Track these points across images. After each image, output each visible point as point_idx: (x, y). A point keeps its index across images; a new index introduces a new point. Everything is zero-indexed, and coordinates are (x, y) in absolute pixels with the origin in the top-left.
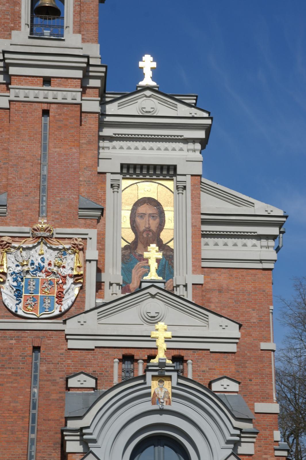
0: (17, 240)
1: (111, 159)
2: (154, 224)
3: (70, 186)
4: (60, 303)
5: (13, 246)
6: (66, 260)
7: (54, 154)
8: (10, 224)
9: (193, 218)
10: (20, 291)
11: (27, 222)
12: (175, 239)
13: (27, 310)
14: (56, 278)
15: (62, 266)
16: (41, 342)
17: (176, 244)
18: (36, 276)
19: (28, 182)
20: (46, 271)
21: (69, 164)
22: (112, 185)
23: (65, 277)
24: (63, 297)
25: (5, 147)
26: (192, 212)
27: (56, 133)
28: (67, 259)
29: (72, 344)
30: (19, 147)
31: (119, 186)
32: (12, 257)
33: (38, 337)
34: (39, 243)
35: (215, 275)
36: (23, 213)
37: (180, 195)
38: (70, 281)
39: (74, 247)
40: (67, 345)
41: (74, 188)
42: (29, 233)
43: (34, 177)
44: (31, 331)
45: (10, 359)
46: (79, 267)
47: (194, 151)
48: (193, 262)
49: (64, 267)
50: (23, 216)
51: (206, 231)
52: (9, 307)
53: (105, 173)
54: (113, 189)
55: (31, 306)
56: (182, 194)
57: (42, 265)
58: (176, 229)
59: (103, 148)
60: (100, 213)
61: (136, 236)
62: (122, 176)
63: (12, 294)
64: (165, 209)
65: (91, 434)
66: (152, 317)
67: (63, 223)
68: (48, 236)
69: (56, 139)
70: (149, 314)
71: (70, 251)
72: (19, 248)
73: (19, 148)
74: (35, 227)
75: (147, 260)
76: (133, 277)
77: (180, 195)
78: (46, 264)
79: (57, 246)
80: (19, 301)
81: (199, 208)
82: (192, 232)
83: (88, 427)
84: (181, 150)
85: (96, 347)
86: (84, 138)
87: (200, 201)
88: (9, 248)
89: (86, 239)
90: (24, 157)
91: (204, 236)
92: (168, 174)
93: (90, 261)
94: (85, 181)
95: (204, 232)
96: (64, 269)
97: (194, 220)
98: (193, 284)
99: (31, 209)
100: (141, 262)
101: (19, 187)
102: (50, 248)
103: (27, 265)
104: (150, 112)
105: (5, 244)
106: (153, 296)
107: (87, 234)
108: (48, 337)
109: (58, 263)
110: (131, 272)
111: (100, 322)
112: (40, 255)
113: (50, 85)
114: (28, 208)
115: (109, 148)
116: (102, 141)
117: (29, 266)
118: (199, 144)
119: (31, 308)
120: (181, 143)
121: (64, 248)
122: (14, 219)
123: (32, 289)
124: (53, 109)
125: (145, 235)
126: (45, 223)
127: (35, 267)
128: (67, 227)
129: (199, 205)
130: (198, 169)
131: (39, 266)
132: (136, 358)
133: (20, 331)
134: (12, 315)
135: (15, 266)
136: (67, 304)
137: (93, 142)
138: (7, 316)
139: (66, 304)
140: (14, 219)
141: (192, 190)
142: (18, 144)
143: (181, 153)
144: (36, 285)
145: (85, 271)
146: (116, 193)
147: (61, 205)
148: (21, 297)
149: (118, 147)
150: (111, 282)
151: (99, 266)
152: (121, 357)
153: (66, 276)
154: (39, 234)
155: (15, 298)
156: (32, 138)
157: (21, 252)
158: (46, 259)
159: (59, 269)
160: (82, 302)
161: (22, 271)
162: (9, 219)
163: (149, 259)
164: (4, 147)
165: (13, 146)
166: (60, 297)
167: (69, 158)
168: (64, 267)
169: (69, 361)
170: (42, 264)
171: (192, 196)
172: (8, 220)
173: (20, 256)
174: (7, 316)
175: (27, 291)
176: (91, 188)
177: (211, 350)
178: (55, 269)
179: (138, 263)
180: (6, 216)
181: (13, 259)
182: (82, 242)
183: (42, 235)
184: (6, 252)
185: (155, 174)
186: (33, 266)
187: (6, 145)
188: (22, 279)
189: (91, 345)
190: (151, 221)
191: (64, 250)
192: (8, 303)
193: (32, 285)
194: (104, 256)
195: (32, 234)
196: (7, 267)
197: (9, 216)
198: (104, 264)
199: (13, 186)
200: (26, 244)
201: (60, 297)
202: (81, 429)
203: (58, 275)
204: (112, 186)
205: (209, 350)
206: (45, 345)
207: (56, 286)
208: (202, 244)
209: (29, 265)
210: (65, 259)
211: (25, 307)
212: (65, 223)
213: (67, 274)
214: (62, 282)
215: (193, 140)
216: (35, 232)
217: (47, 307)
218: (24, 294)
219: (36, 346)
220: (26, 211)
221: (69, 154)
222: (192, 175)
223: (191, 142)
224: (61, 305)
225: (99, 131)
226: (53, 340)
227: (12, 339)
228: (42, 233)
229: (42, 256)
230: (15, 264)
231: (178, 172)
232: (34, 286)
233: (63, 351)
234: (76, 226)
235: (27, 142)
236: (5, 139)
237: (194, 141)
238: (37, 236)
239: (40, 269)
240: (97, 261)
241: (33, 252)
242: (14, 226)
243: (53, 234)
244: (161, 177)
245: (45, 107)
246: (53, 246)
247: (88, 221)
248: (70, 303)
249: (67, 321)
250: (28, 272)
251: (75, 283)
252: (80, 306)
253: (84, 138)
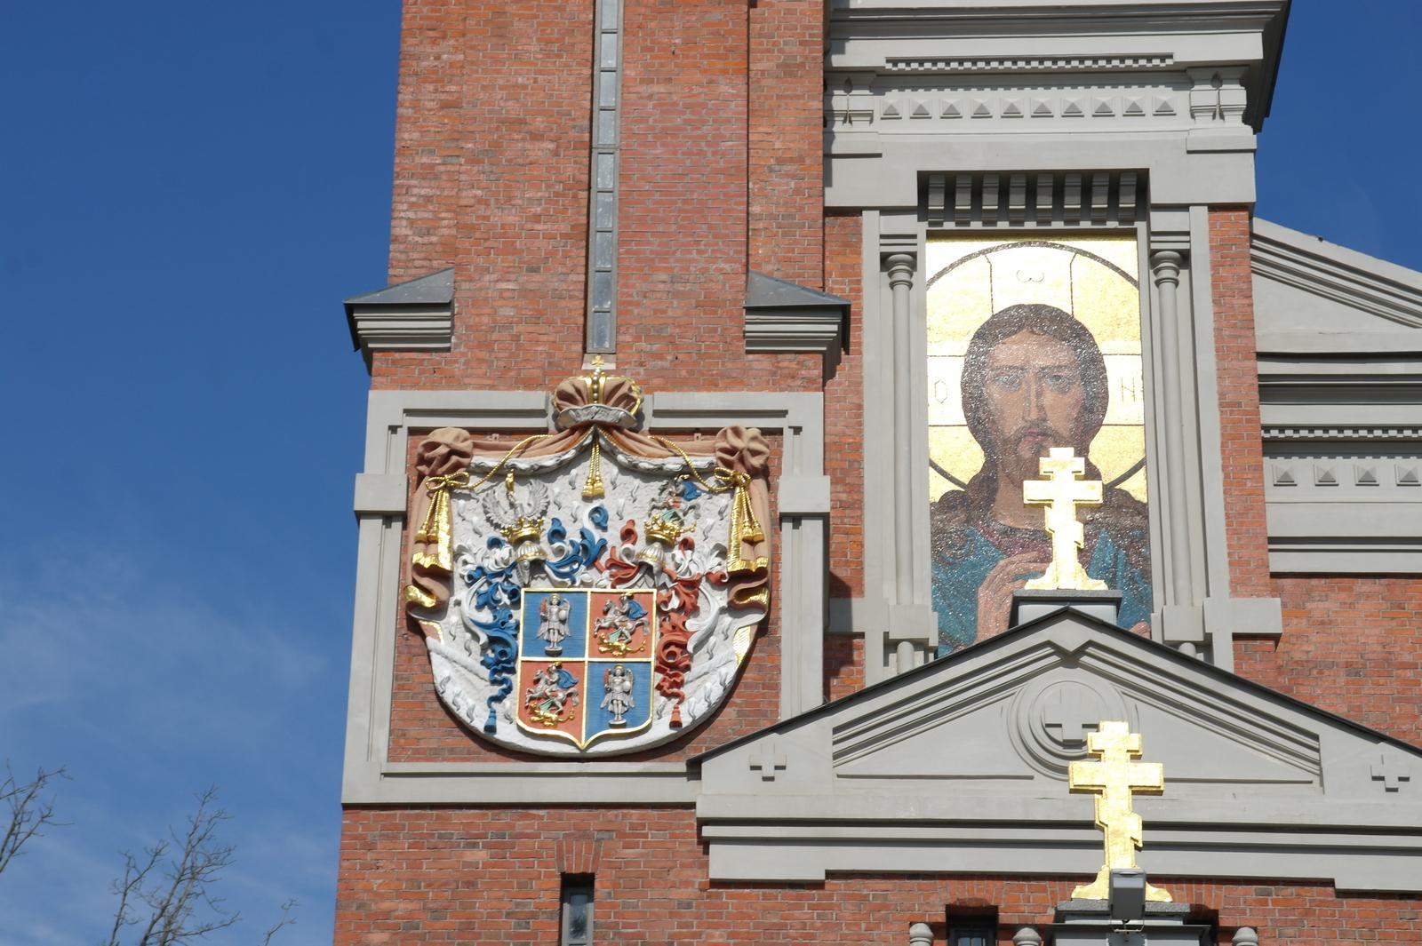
0: (497, 442)
1: (879, 155)
2: (1060, 409)
3: (710, 227)
4: (672, 689)
5: (477, 466)
6: (697, 516)
7: (645, 105)
8: (467, 381)
9: (1222, 373)
10: (507, 644)
11: (537, 373)
12: (1151, 462)
13: (534, 723)
14: (655, 591)
15: (680, 539)
16: (597, 854)
17: (1156, 483)
18: (574, 582)
19: (537, 218)
20: (613, 564)
21: (703, 144)
22: (884, 258)
23: (692, 585)
24: (688, 668)
25: (450, 98)
26: (1217, 350)
27: (652, 25)
28: (701, 511)
29: (726, 862)
30: (501, 82)
31: (913, 263)
32: (472, 511)
33: (583, 835)
34: (584, 453)
35: (1325, 603)
36: (516, 338)
37: (1168, 286)
38: (711, 602)
39: (729, 464)
40: (706, 865)
41: (727, 236)
42: (541, 413)
43: (564, 196)
44: (552, 811)
46: (752, 542)
47: (1219, 112)
48: (1229, 546)
49: (687, 545)
50: (518, 349)
51: (1282, 428)
52: (462, 714)
53: (856, 212)
54: (890, 275)
55: (553, 705)
56: (1176, 283)
57: (597, 540)
58: (1155, 424)
59: (848, 117)
60: (835, 328)
61: (987, 446)
62: (924, 226)
63: (474, 660)
64: (1103, 348)
66: (1067, 744)
67: (684, 373)
68: (620, 420)
69: (650, 50)
70: (1053, 732)
71: (711, 482)
72: (498, 474)
73: (501, 88)
74: (566, 386)
75: (1039, 508)
76: (980, 615)
77: (1168, 286)
78: (613, 537)
79: (659, 461)
80: (504, 686)
81: (1249, 333)
82: (1224, 428)
84: (1165, 111)
85: (831, 874)
86: (768, 51)
87: (1251, 305)
88: (461, 471)
89: (779, 432)
90: (522, 122)
91: (1274, 447)
92: (1113, 210)
93: (796, 519)
94: (772, 217)
95: (1274, 433)
96: (689, 552)
97: (1227, 382)
98: (1236, 637)
99: (549, 323)
100: (1014, 559)
101: (504, 235)
102: (631, 470)
103: (534, 539)
105: (446, 458)
106: (1070, 659)
107: (783, 414)
108: (625, 836)
109: (663, 527)
110: (972, 597)
111: (843, 770)
112: (587, 499)
114: (538, 316)
115: (869, 115)
116: (842, 92)
117: (544, 543)
118: (1238, 86)
119: (551, 711)
120: (1162, 87)
121: (686, 469)
122: (481, 361)
123: (555, 638)
126: (607, 373)
127: (569, 549)
128: (698, 387)
129: (1249, 323)
130: (1239, 182)
131: (586, 542)
132: (1005, 918)
133: (509, 812)
134: (473, 745)
135: (485, 546)
136: (701, 693)
137: (802, 65)
138: (452, 751)
139: (700, 695)
140: (481, 361)
141: (1215, 266)
142: (498, 72)
143: (1165, 123)
144: (573, 620)
145: (775, 557)
146: (901, 288)
147: (675, 302)
148: (513, 671)
149: (906, 112)
150: (892, 636)
151: (841, 573)
152: (940, 916)
153: (699, 581)
154: (582, 413)
155: (486, 672)
156: (556, 47)
157: (510, 488)
158: (612, 514)
159: (668, 555)
160: (765, 686)
161: (514, 566)
162: (463, 360)
163: (1046, 508)
164: (443, 97)
165: (478, 80)
166: (674, 665)
167: (706, 117)
168: (687, 545)
169: (717, 933)
170: (597, 535)
171: (1215, 286)
172: (458, 368)
173: (505, 503)
174: (452, 751)
175: (534, 644)
176: (797, 242)
177: (1340, 885)
178: (651, 555)
179: (1002, 563)
180: (448, 350)
181: (478, 519)
182: (762, 442)
183: (597, 418)
184: (449, 488)
185: (1058, 211)
186: (557, 544)
187: (453, 88)
188: (514, 594)
189: (808, 863)
191: (686, 477)
192: (458, 695)
193: (554, 618)
194: (860, 532)
195: (555, 417)
196: (450, 548)
197: (463, 349)
198: (861, 564)
199: (478, 235)
200: (530, 456)
201: (672, 666)
203: (664, 579)
204: (886, 261)
205: (1330, 883)
206: (610, 865)
207: (656, 620)
208: (1269, 478)
209: (544, 538)
210: (691, 514)
211: (528, 710)
212: (691, 372)
213: (702, 572)
214: (682, 607)
215: (1211, 73)
216: (567, 406)
217: (619, 709)
218: (521, 658)
219: (574, 872)
220: (530, 329)
221: (704, 106)
222: (1213, 208)
223: (1203, 81)
224: (677, 700)
225: (827, 53)
226: (645, 845)
227: (475, 846)
228: (594, 406)
229: (596, 504)
230: (485, 539)
231: (1156, 197)
232: (563, 622)
233: (690, 892)
234: (735, 382)
235: (536, 65)
236: (452, 65)
237: (1216, 73)
238: (574, 424)
239: (588, 554)
240: (825, 517)
241: (559, 486)
242: (481, 387)
243: (640, 416)
244: (1085, 225)
246: (641, 459)
247: (787, 362)
248: (717, 693)
249: (706, 766)
250: (537, 566)
251: (733, 609)
252: (757, 704)
253: (768, 51)
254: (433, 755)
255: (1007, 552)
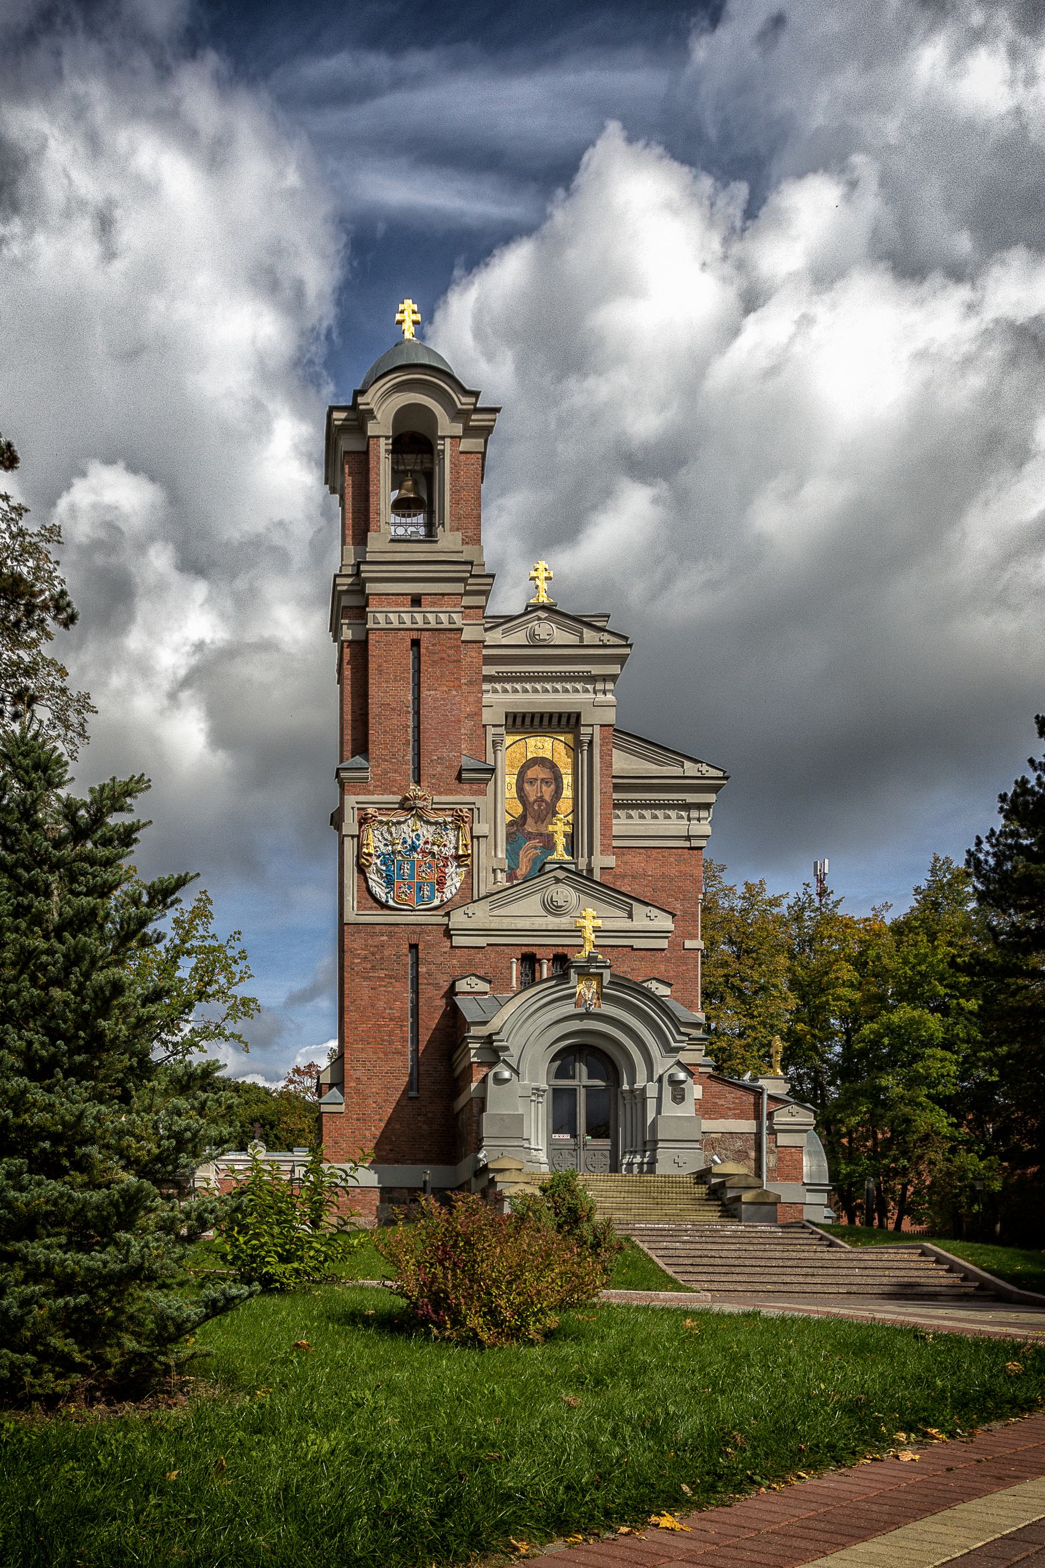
2: (548, 792)
29: (458, 941)
33: (415, 933)
45: (382, 958)
65: (502, 1041)
78: (421, 842)
83: (498, 1034)
84: (587, 691)
93: (478, 837)
104: (545, 640)
107: (474, 804)
113: (420, 606)
124: (425, 638)
125: (536, 808)
139: (450, 891)
166: (441, 883)
168: (445, 846)
190: (544, 788)
202: (491, 1035)
222: (601, 726)
234: (458, 793)
241: (404, 827)
245: (415, 635)
247: (475, 787)
254: (371, 908)
255: (530, 839)
